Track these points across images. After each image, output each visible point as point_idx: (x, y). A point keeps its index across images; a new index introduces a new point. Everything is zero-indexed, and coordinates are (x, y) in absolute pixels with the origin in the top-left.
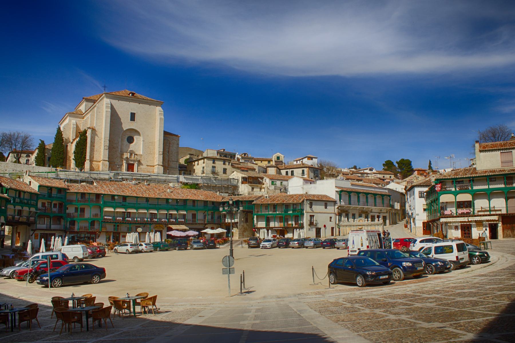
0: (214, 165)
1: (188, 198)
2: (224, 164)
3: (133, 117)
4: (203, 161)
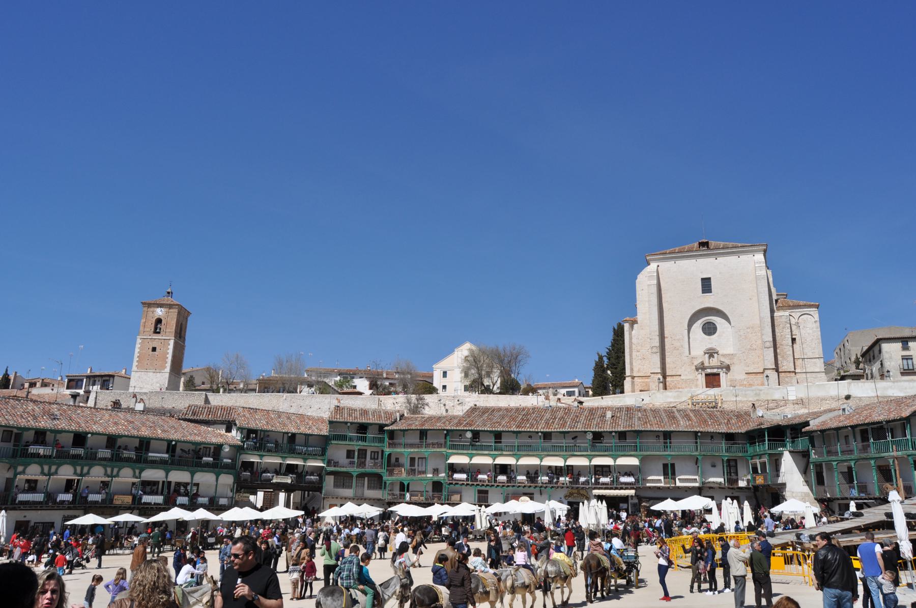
3: (706, 285)
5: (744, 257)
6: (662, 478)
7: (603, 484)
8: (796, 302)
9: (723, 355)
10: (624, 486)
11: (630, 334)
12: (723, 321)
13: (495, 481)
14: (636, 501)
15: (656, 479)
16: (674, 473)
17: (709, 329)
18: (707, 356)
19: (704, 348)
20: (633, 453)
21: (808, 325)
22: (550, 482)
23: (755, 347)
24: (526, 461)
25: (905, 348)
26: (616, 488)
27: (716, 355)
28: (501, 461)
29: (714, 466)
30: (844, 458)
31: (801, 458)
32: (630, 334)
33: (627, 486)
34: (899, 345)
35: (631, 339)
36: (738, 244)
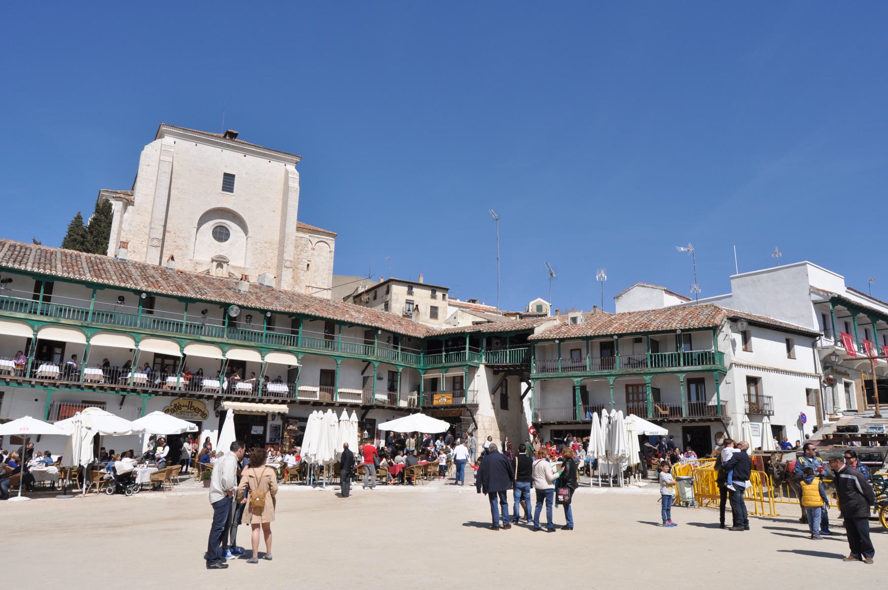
0: (410, 298)
1: (306, 312)
2: (433, 297)
3: (229, 182)
4: (385, 288)
5: (275, 164)
6: (317, 389)
7: (242, 392)
8: (315, 228)
9: (233, 267)
10: (273, 398)
11: (122, 217)
12: (238, 228)
13: (33, 375)
14: (278, 422)
15: (310, 389)
16: (333, 384)
17: (221, 234)
18: (215, 264)
19: (213, 255)
20: (291, 348)
21: (322, 253)
22: (151, 383)
23: (269, 265)
24: (102, 340)
25: (410, 293)
26: (261, 401)
27: (225, 265)
28: (49, 334)
29: (380, 378)
30: (564, 374)
31: (491, 374)
32: (122, 217)
33: (277, 398)
34: (405, 289)
35: (121, 223)
36: (270, 144)
